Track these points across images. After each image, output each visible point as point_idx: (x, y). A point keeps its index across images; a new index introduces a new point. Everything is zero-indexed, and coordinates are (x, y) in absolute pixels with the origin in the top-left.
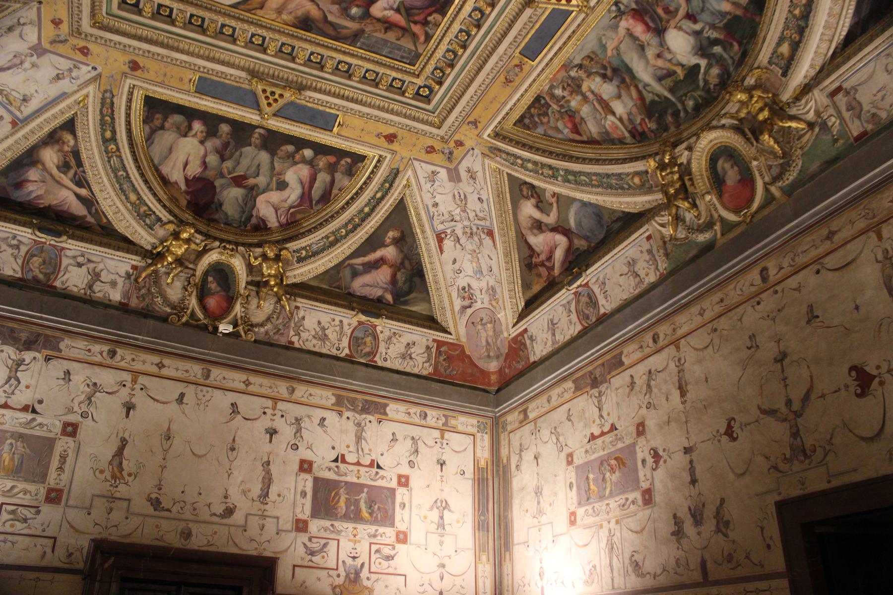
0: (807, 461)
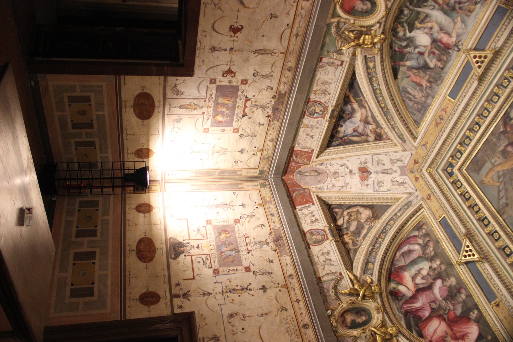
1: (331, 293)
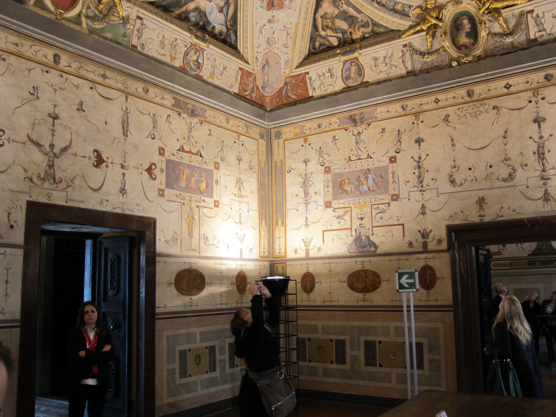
0: (55, 185)
1: (428, 60)
